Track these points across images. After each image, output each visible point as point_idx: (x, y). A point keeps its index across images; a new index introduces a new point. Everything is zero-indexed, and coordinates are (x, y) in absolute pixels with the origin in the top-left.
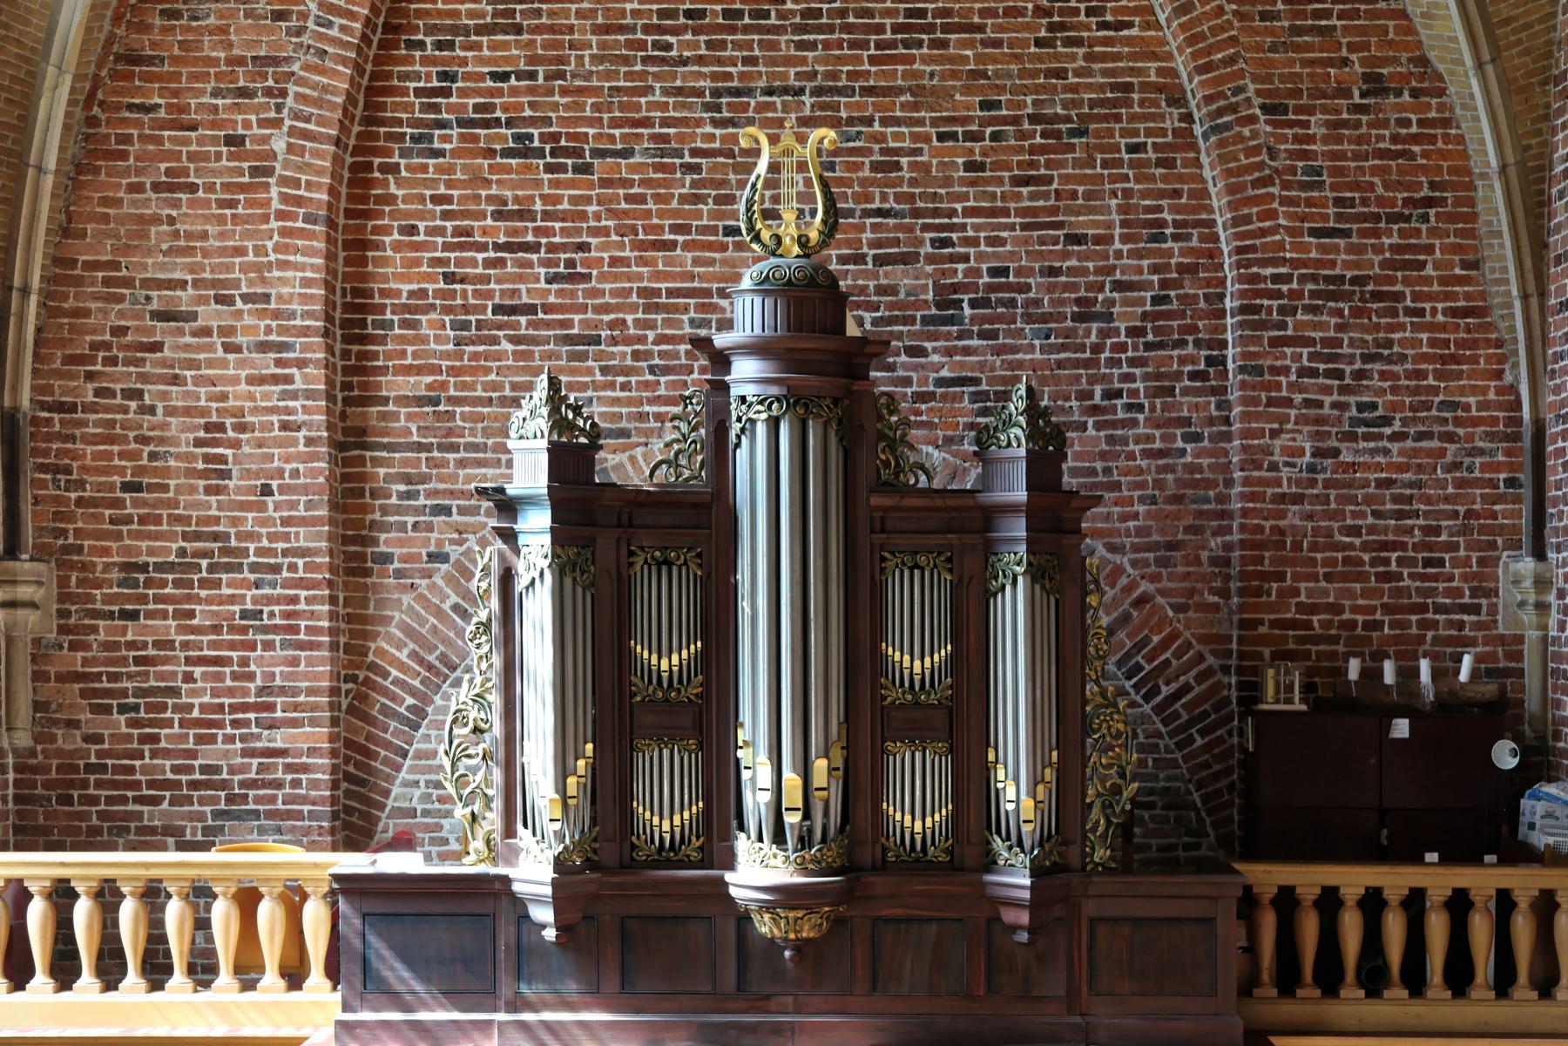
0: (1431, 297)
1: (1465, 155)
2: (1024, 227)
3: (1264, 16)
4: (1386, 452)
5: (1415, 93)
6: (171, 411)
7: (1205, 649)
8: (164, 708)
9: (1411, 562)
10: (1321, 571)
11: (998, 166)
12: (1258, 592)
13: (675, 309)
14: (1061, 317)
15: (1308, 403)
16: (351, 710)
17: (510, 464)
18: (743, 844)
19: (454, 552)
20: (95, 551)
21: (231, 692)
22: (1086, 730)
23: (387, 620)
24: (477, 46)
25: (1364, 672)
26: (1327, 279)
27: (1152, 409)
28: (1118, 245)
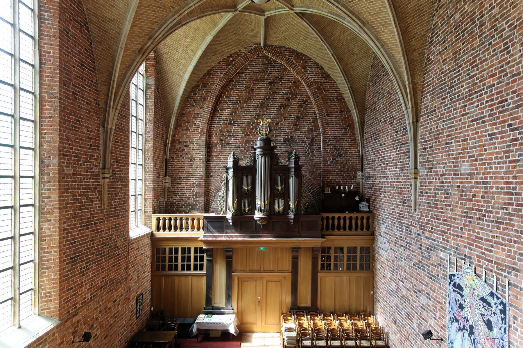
0: (348, 138)
1: (353, 120)
3: (327, 103)
5: (346, 112)
9: (345, 173)
11: (291, 123)
13: (249, 143)
14: (299, 143)
15: (332, 153)
16: (207, 195)
18: (256, 212)
19: (220, 175)
21: (192, 193)
22: (302, 196)
23: (212, 184)
24: (225, 111)
25: (338, 188)
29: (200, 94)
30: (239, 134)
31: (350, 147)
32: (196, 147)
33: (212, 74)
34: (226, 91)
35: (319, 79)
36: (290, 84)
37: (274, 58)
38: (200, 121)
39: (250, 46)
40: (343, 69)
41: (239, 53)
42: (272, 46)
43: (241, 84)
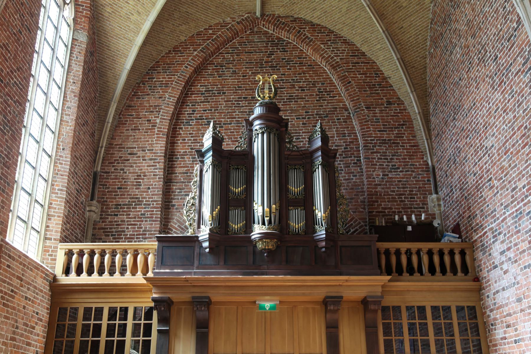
1: (410, 116)
3: (364, 91)
4: (399, 175)
5: (398, 104)
7: (361, 221)
8: (121, 235)
9: (407, 198)
10: (387, 200)
11: (309, 124)
12: (372, 205)
15: (380, 165)
20: (110, 202)
21: (137, 231)
24: (200, 105)
26: (382, 140)
27: (345, 170)
28: (336, 138)
29: (160, 78)
31: (411, 157)
32: (148, 156)
33: (181, 51)
34: (201, 77)
35: (348, 58)
36: (303, 68)
38: (158, 117)
39: (240, 16)
41: (224, 25)
42: (274, 15)
43: (226, 69)
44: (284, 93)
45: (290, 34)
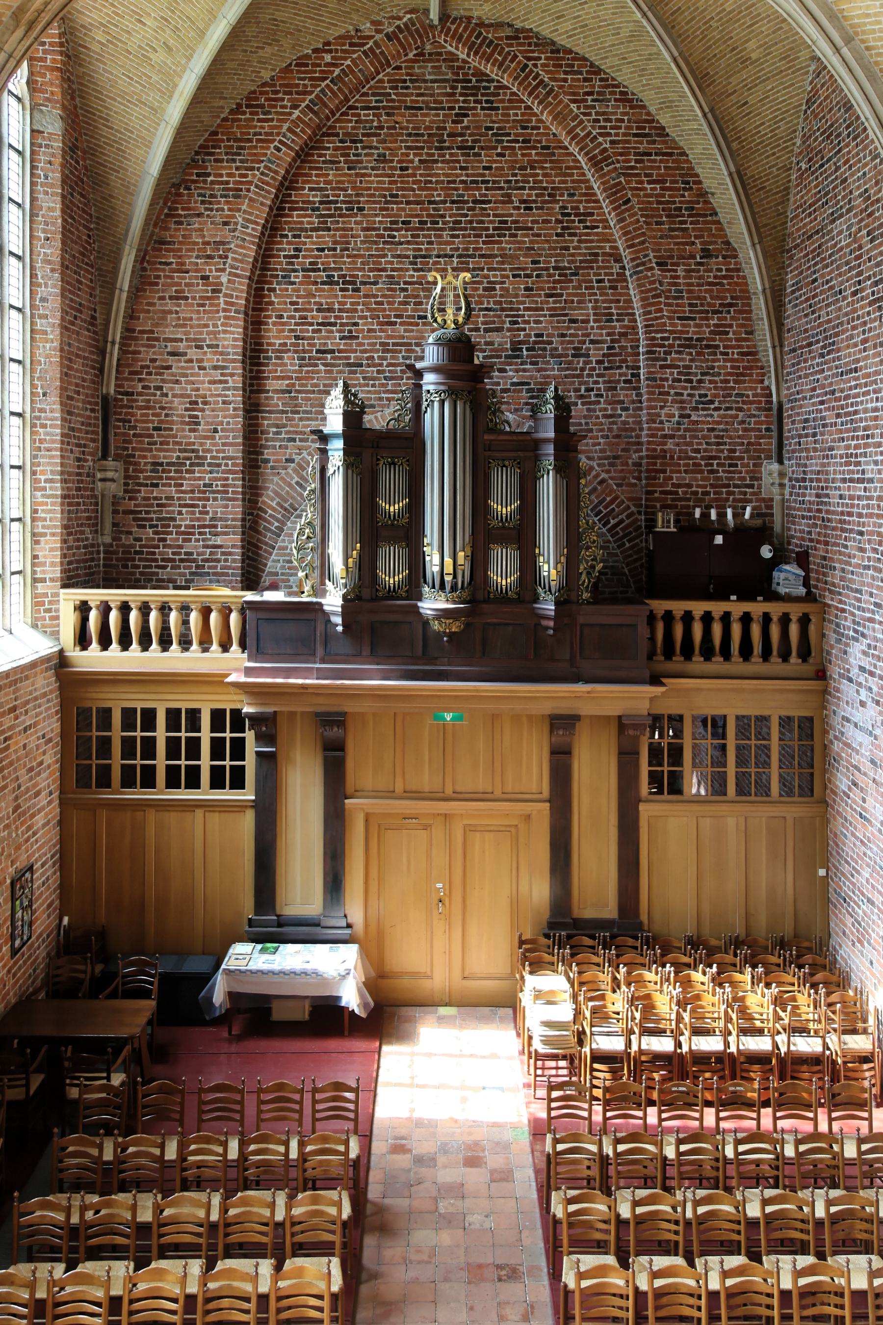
1: (746, 284)
2: (551, 316)
3: (657, 223)
4: (712, 416)
5: (724, 257)
6: (174, 396)
7: (630, 504)
8: (169, 526)
9: (723, 465)
10: (682, 469)
11: (539, 289)
12: (655, 478)
13: (396, 351)
14: (567, 356)
15: (677, 394)
16: (251, 528)
17: (324, 419)
19: (297, 458)
20: (140, 457)
21: (198, 519)
23: (267, 488)
24: (311, 237)
26: (686, 339)
28: (592, 324)
29: (221, 176)
30: (361, 318)
31: (739, 376)
32: (209, 360)
33: (262, 106)
34: (311, 168)
35: (628, 142)
36: (530, 155)
37: (474, 62)
38: (224, 270)
39: (393, 18)
40: (712, 110)
41: (356, 40)
42: (469, 18)
43: (363, 148)
44: (489, 215)
45: (504, 72)
